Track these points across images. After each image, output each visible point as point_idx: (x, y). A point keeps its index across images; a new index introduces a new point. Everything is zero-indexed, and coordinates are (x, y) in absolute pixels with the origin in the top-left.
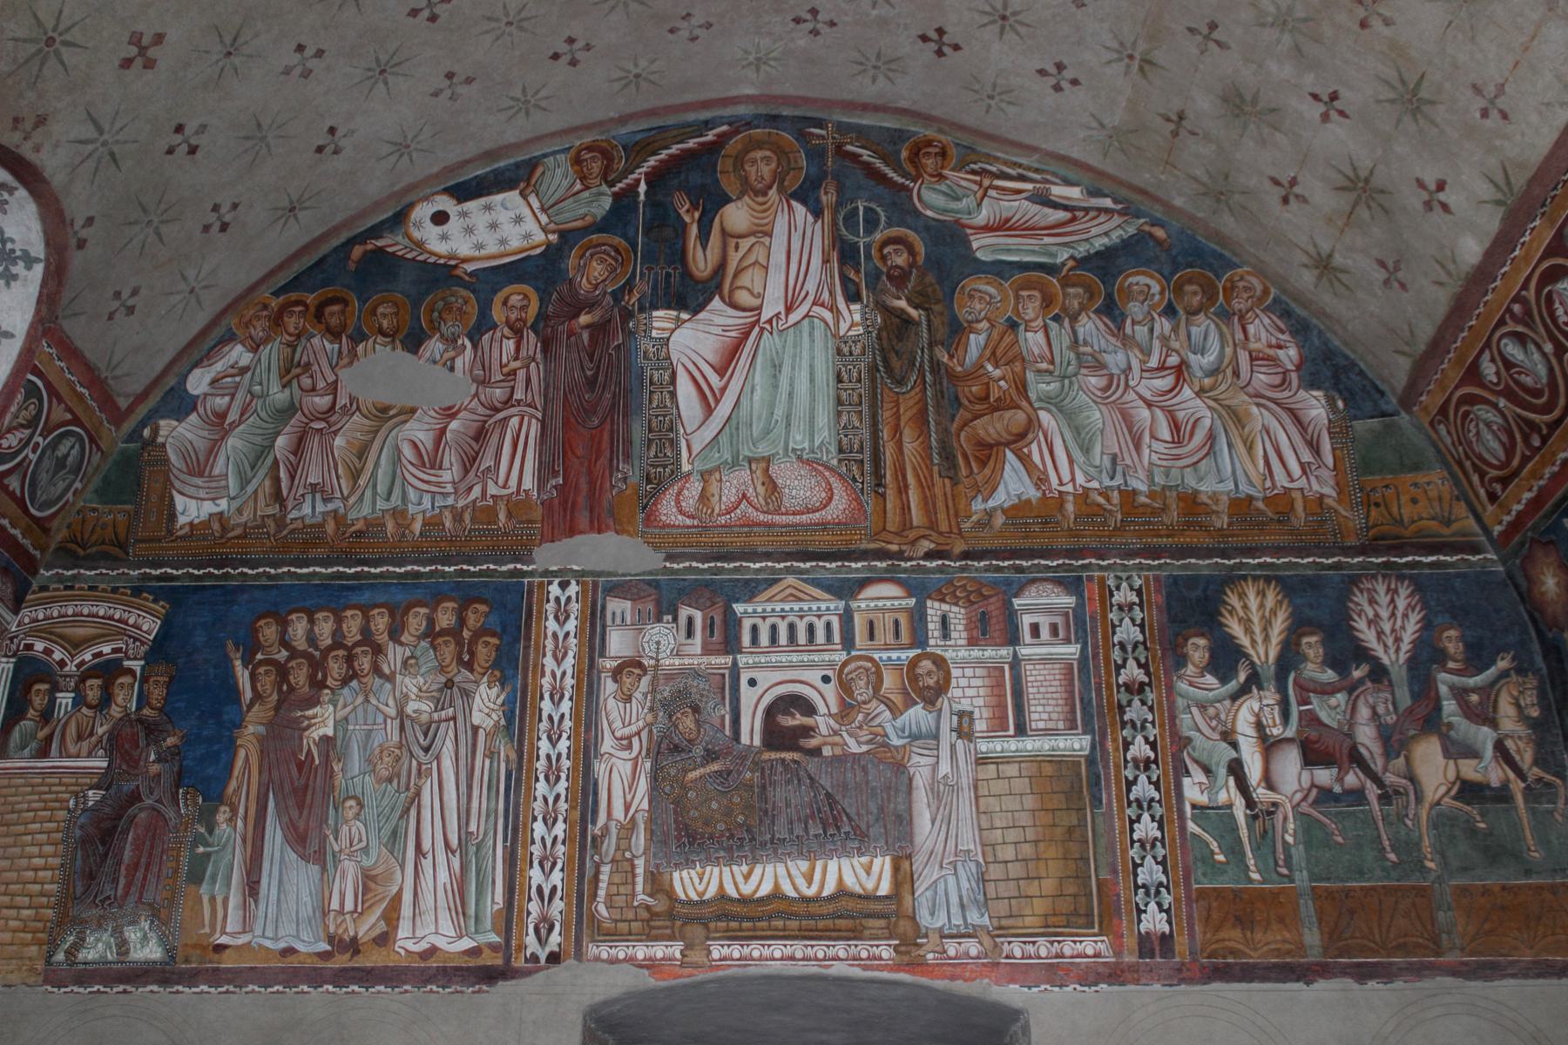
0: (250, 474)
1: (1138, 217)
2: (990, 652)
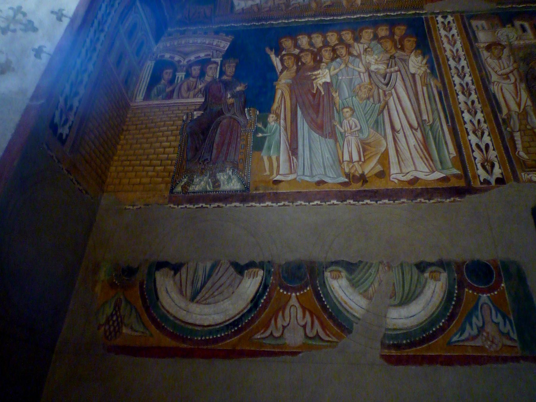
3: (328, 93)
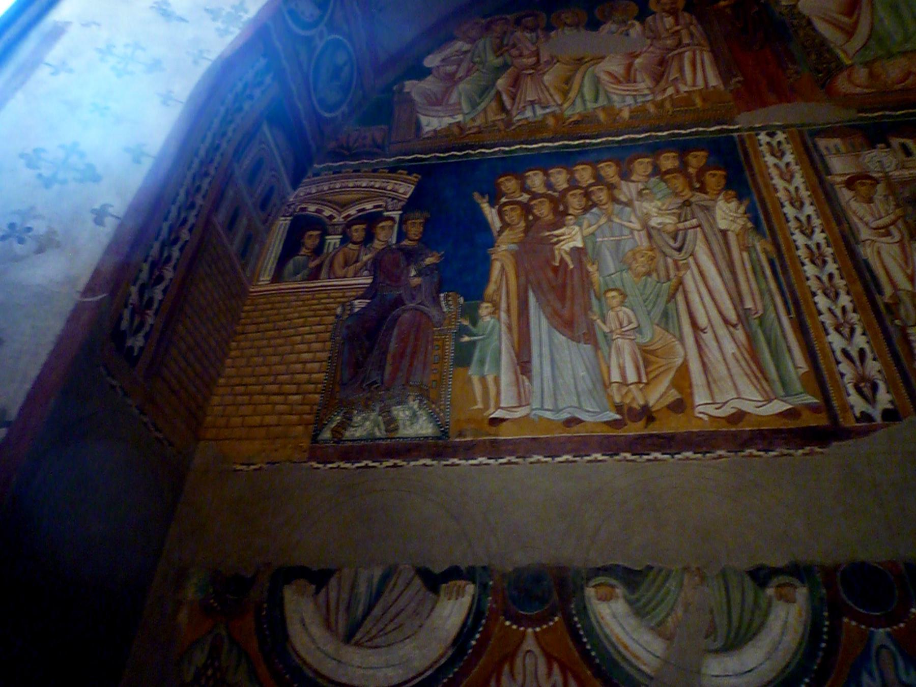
0: (478, 101)
3: (580, 264)
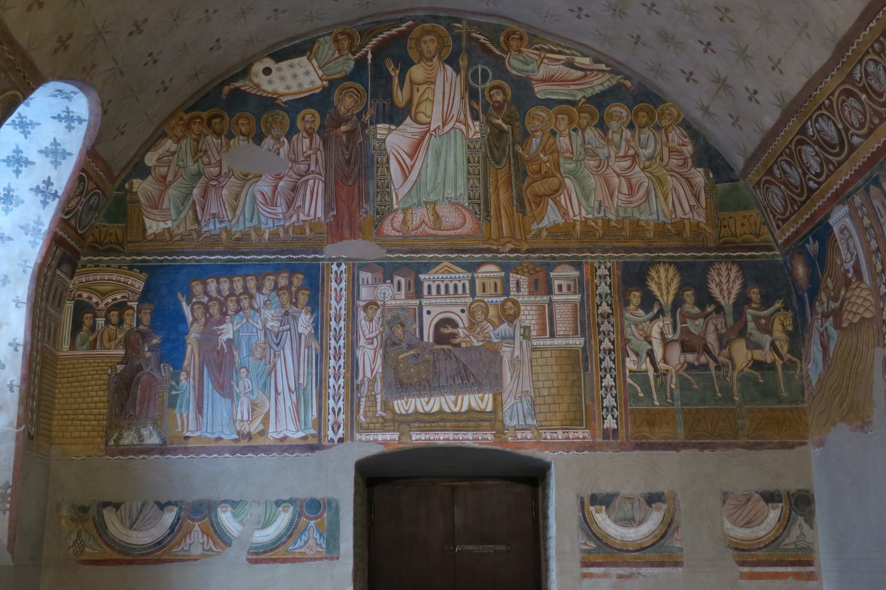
0: (181, 208)
1: (618, 75)
2: (539, 298)
